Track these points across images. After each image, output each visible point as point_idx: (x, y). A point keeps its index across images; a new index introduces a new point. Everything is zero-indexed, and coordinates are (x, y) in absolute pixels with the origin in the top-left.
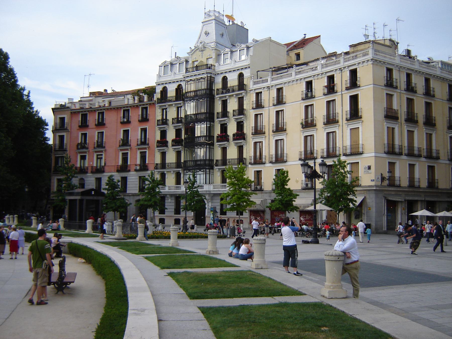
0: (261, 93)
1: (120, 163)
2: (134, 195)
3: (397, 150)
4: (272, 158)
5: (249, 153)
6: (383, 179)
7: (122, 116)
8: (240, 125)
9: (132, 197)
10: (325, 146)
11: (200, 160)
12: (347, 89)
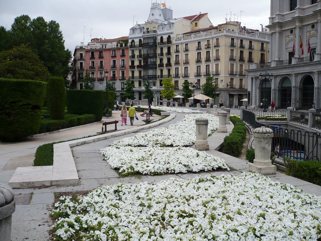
0: (178, 45)
1: (112, 76)
2: (119, 91)
3: (234, 73)
4: (183, 75)
5: (173, 72)
6: (227, 85)
8: (169, 60)
9: (118, 92)
10: (205, 71)
11: (151, 75)
12: (215, 47)
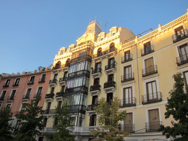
7: (30, 80)
8: (111, 77)
